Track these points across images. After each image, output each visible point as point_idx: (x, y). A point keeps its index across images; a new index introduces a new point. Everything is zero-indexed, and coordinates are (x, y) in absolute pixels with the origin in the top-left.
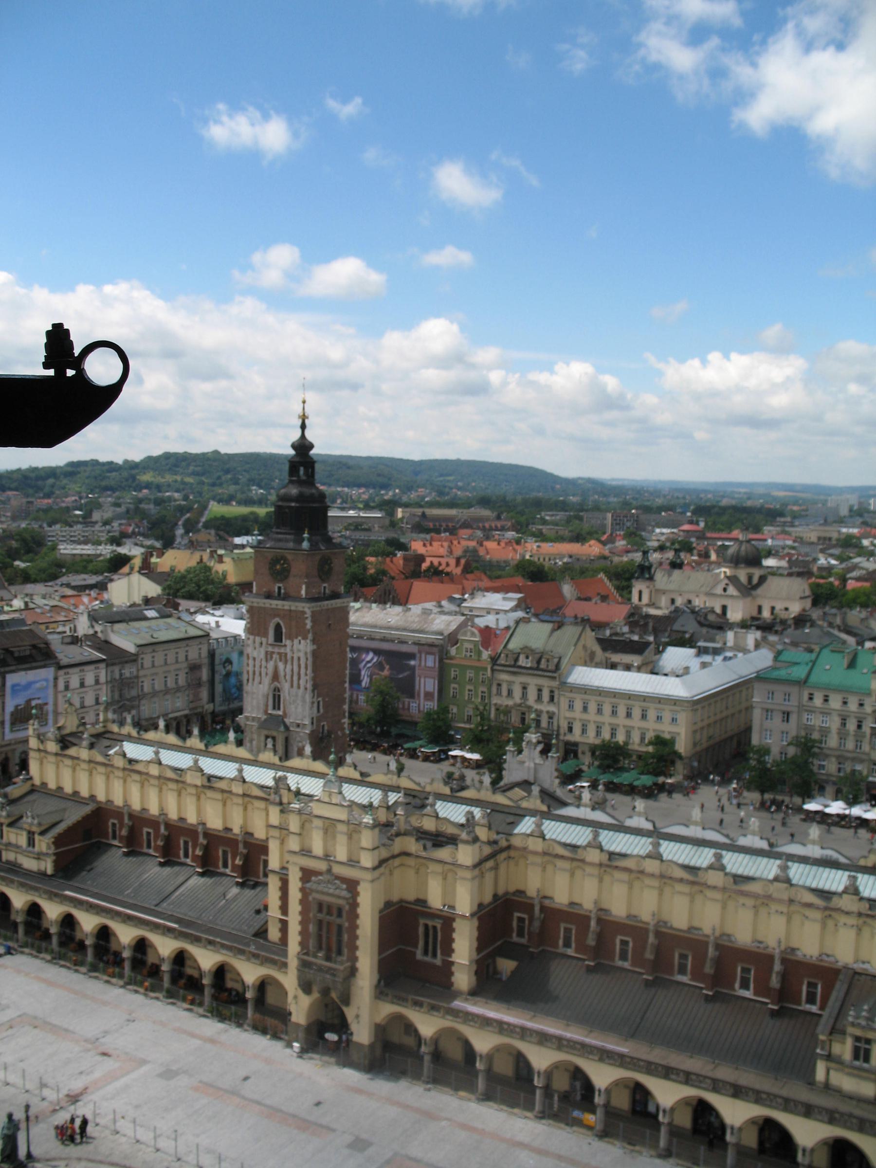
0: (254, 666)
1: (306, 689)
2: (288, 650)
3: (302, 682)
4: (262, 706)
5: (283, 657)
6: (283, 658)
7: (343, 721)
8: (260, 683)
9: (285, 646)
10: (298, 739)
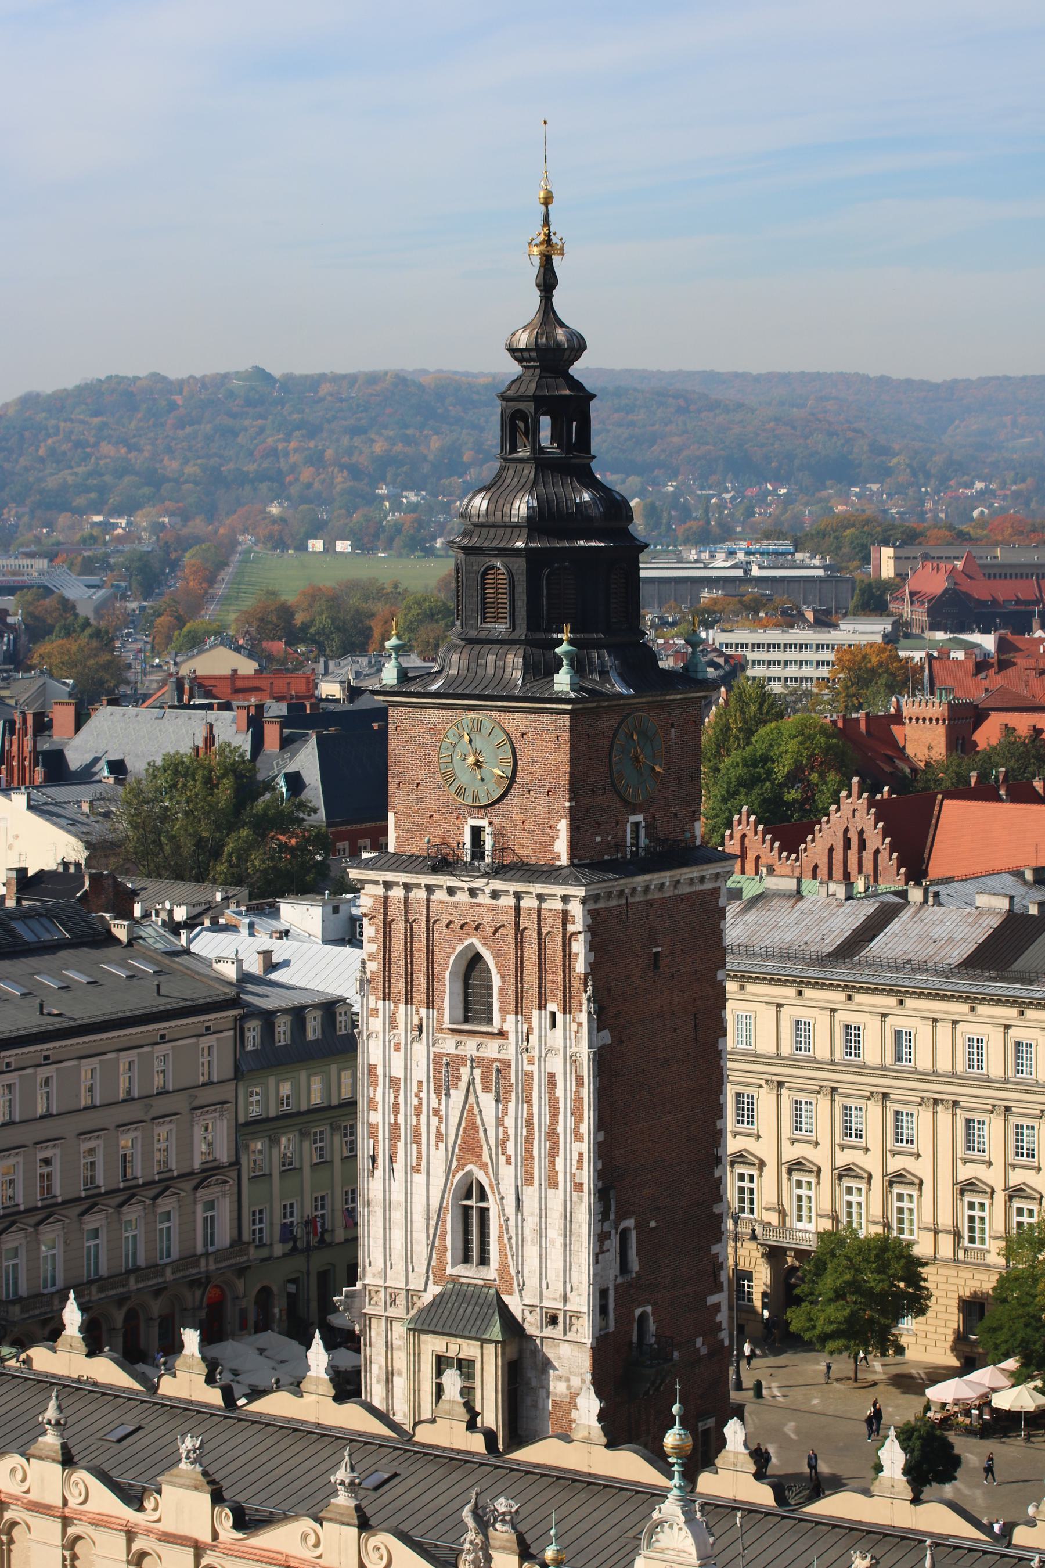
5: (498, 1077)
7: (712, 1300)
8: (417, 1169)
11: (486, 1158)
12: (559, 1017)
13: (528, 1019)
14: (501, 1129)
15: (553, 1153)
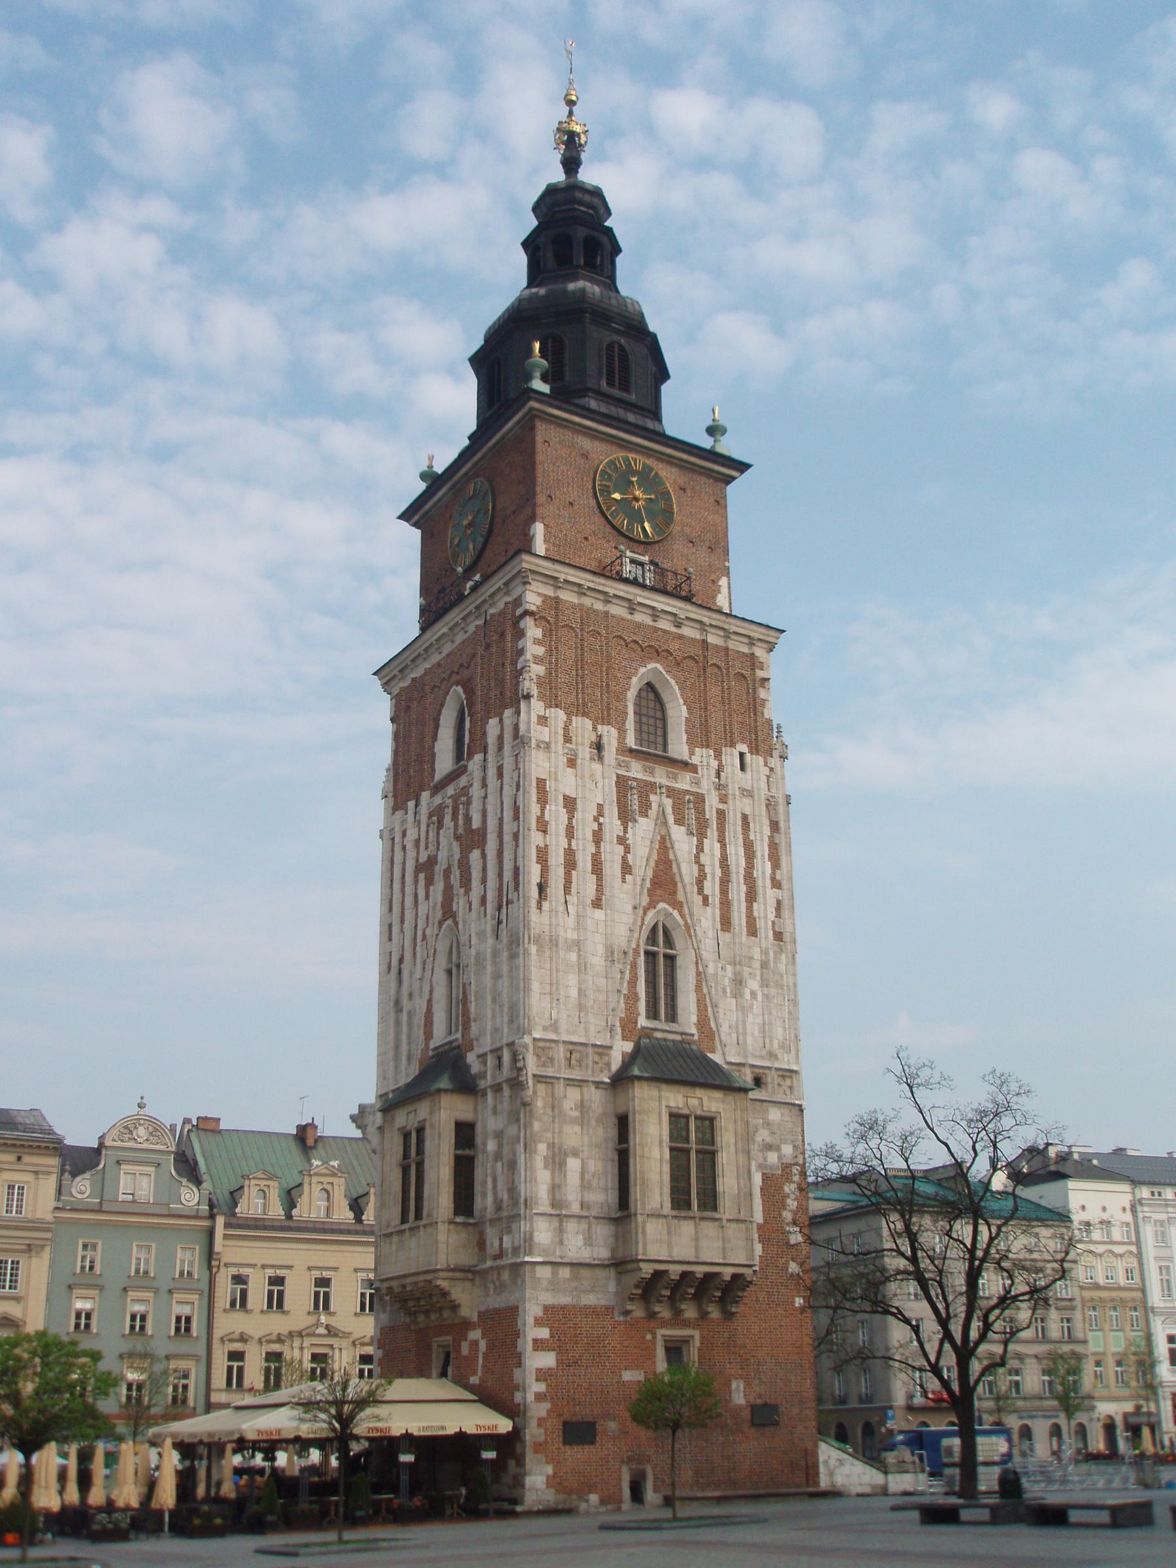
0: (570, 833)
1: (778, 936)
2: (706, 784)
3: (765, 910)
5: (688, 807)
6: (691, 815)
8: (597, 904)
9: (693, 768)
10: (763, 1135)
11: (680, 896)
12: (748, 757)
13: (718, 755)
14: (695, 868)
15: (751, 896)
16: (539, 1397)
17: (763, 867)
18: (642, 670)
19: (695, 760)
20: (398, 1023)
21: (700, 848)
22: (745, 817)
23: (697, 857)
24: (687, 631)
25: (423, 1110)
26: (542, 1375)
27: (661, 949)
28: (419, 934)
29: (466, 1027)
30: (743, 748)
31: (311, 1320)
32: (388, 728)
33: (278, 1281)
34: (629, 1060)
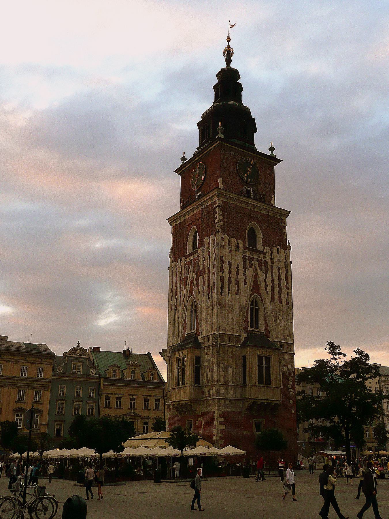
0: (230, 272)
1: (288, 303)
2: (268, 258)
3: (284, 296)
4: (242, 322)
5: (263, 265)
6: (263, 267)
8: (237, 294)
9: (264, 253)
10: (283, 362)
15: (280, 291)
16: (221, 438)
17: (284, 283)
18: (250, 224)
19: (265, 251)
20: (174, 326)
21: (266, 277)
22: (279, 268)
23: (265, 280)
24: (263, 212)
25: (185, 353)
26: (221, 431)
27: (254, 307)
28: (182, 300)
29: (198, 329)
30: (279, 247)
31: (128, 411)
32: (171, 237)
33: (119, 399)
34: (246, 339)
